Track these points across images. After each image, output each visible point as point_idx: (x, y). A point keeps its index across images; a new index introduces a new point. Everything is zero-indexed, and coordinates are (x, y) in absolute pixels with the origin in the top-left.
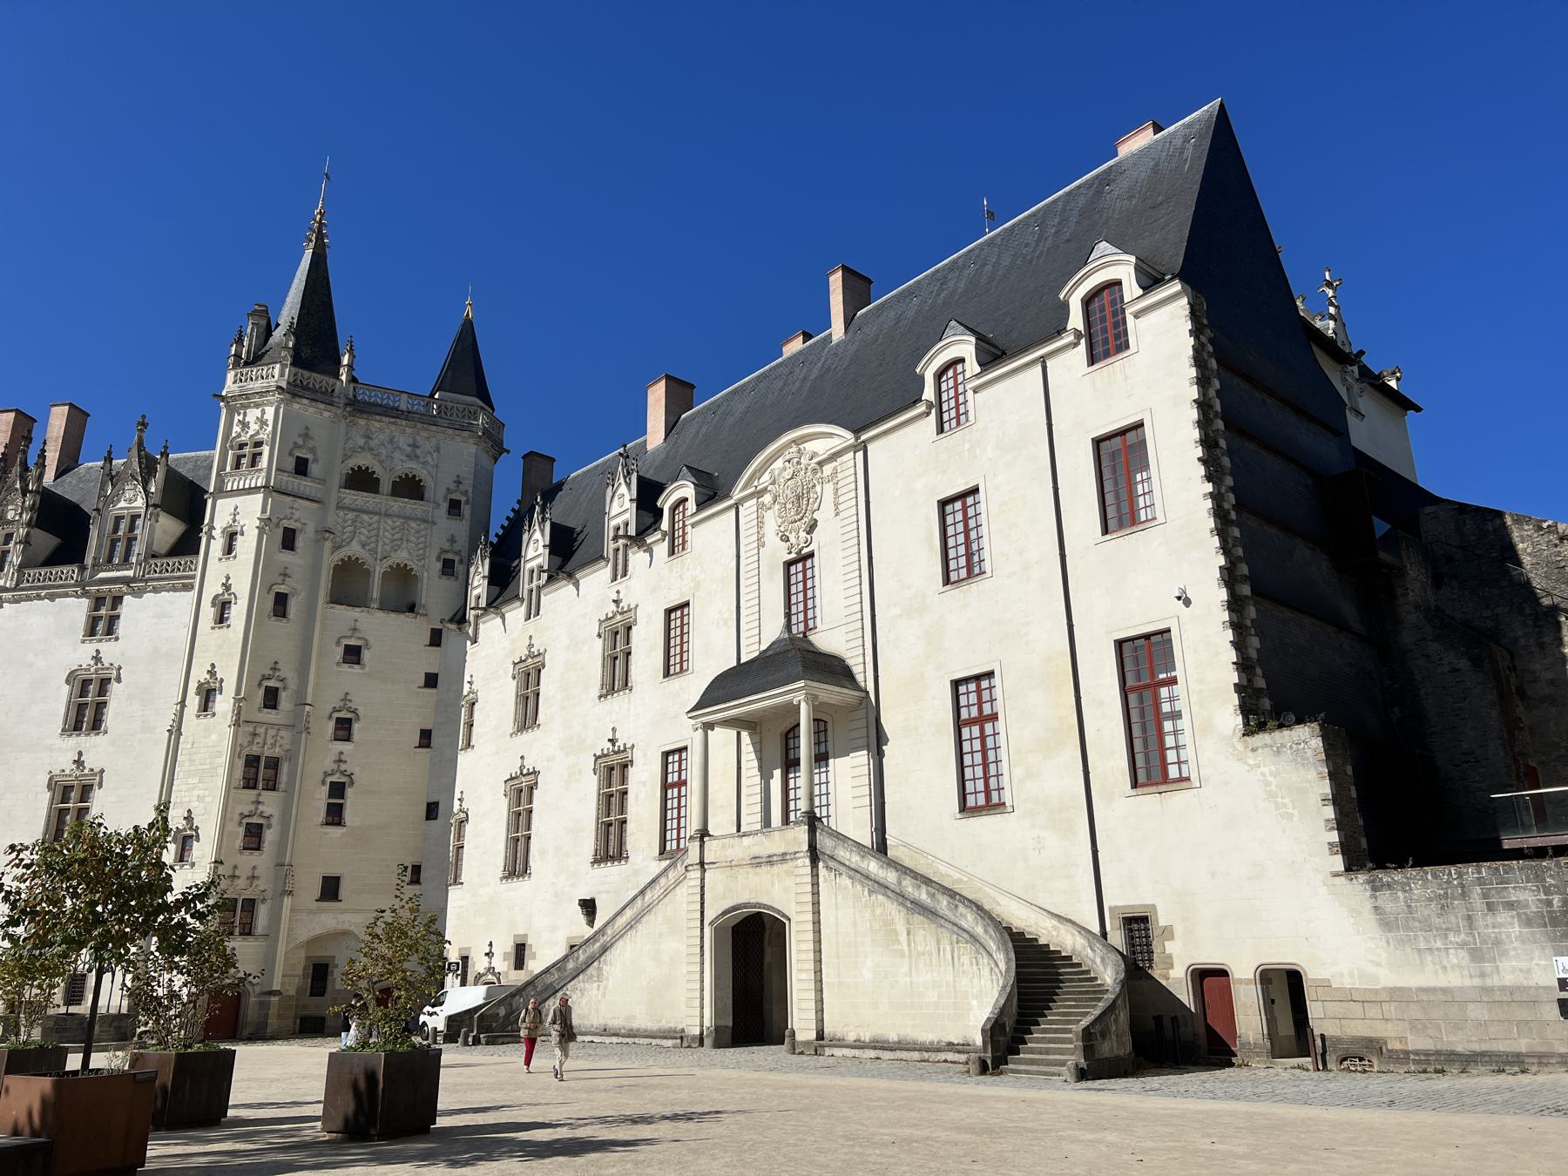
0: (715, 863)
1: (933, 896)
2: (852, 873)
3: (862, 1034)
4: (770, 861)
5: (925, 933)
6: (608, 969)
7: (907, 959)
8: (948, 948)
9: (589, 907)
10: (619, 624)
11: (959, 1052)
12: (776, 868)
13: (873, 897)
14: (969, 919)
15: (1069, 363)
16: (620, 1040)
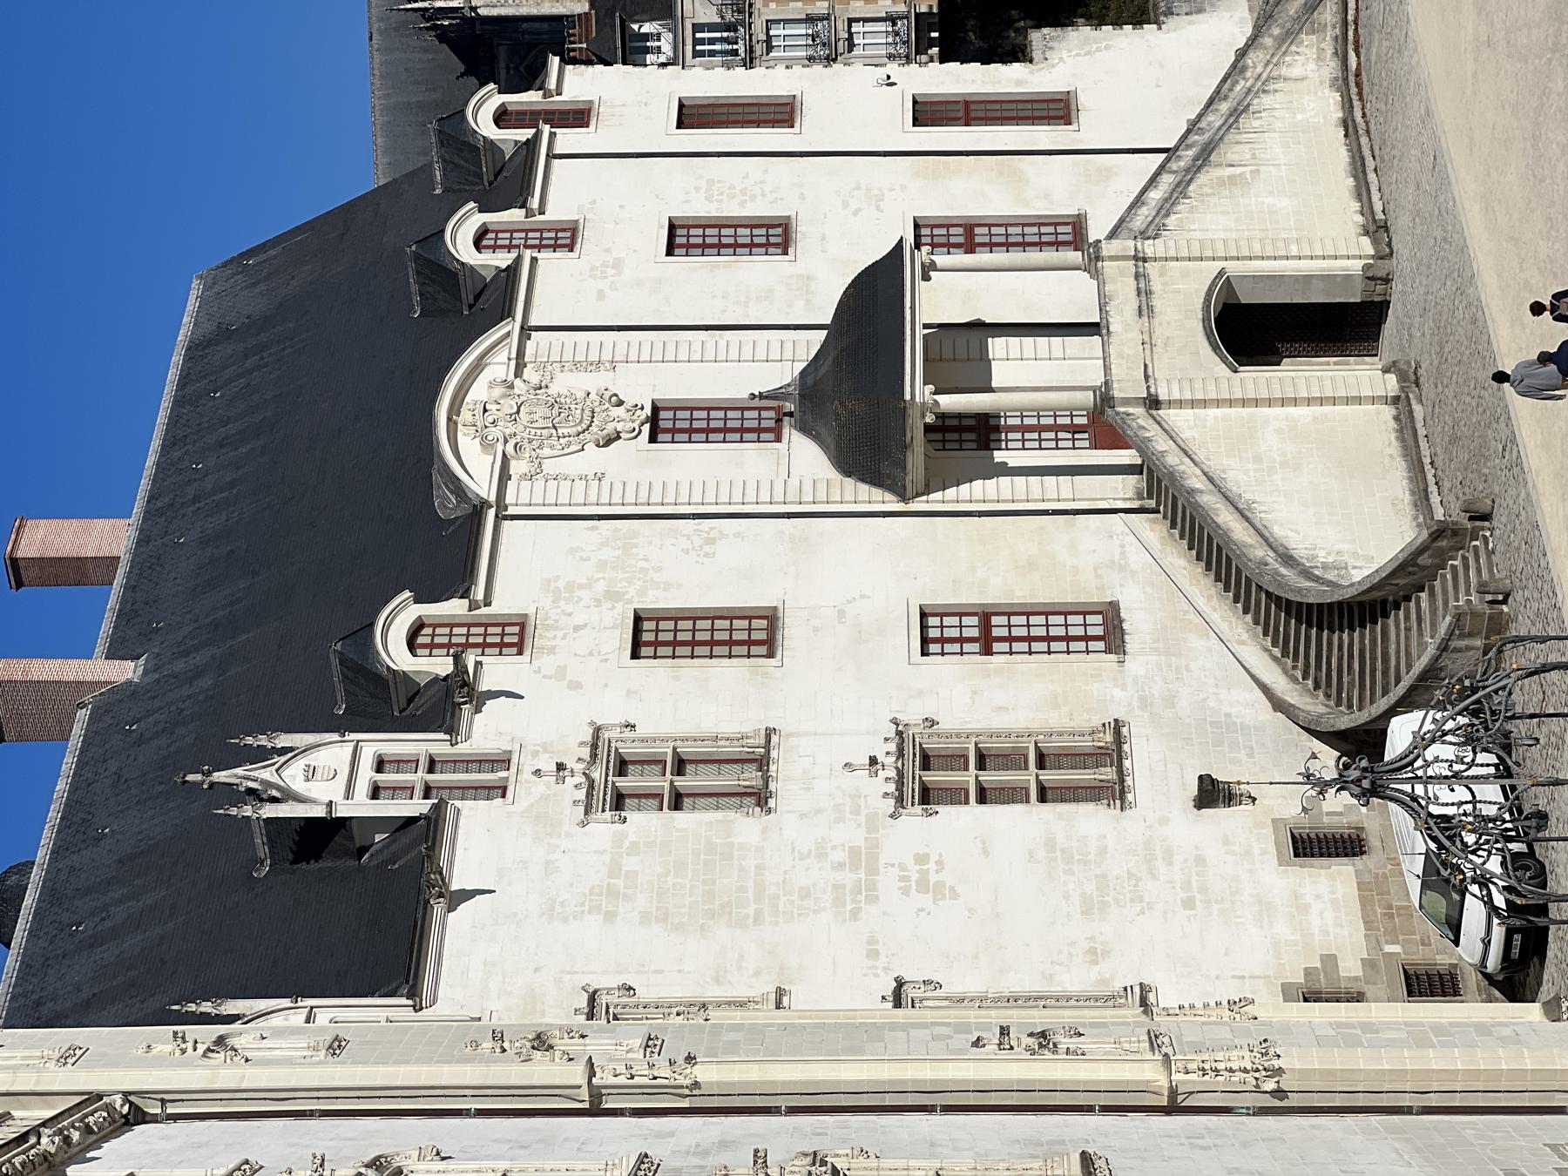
0: (1146, 366)
1: (1189, 147)
2: (1163, 212)
3: (1355, 209)
4: (1145, 293)
5: (1231, 151)
6: (1322, 554)
7: (1262, 168)
8: (1244, 136)
9: (1212, 793)
10: (610, 778)
11: (1352, 107)
12: (1156, 285)
13: (1192, 195)
14: (1214, 120)
15: (568, 139)
16: (1433, 488)
